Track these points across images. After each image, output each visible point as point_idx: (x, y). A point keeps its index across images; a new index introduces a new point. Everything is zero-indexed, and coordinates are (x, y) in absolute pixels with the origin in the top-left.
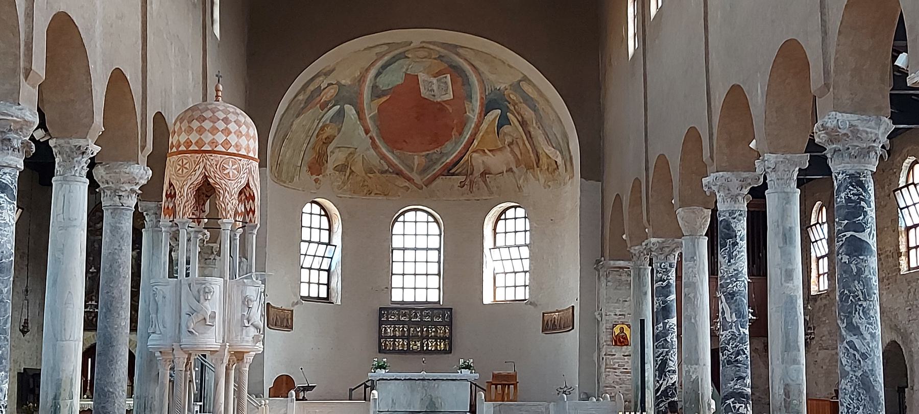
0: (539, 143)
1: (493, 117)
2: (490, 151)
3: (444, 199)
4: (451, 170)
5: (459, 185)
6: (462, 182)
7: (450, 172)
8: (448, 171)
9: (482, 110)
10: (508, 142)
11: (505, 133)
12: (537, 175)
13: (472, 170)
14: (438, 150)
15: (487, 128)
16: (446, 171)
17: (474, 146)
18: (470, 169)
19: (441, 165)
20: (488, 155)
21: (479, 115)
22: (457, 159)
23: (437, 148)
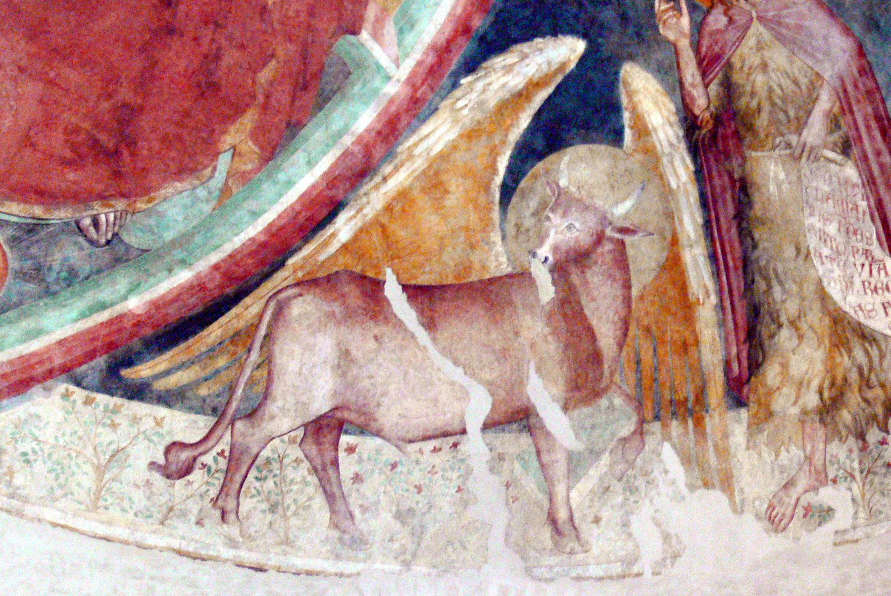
0: (803, 253)
1: (516, 81)
2: (414, 292)
3: (51, 514)
4: (129, 362)
5: (161, 460)
6: (183, 446)
7: (124, 372)
8: (113, 370)
9: (463, 29)
10: (556, 249)
11: (560, 193)
12: (723, 453)
13: (260, 389)
14: (106, 216)
15: (454, 147)
16: (101, 361)
17: (325, 244)
18: (251, 382)
19: (83, 316)
20: (400, 325)
21: (431, 59)
22: (196, 305)
23: (103, 197)
